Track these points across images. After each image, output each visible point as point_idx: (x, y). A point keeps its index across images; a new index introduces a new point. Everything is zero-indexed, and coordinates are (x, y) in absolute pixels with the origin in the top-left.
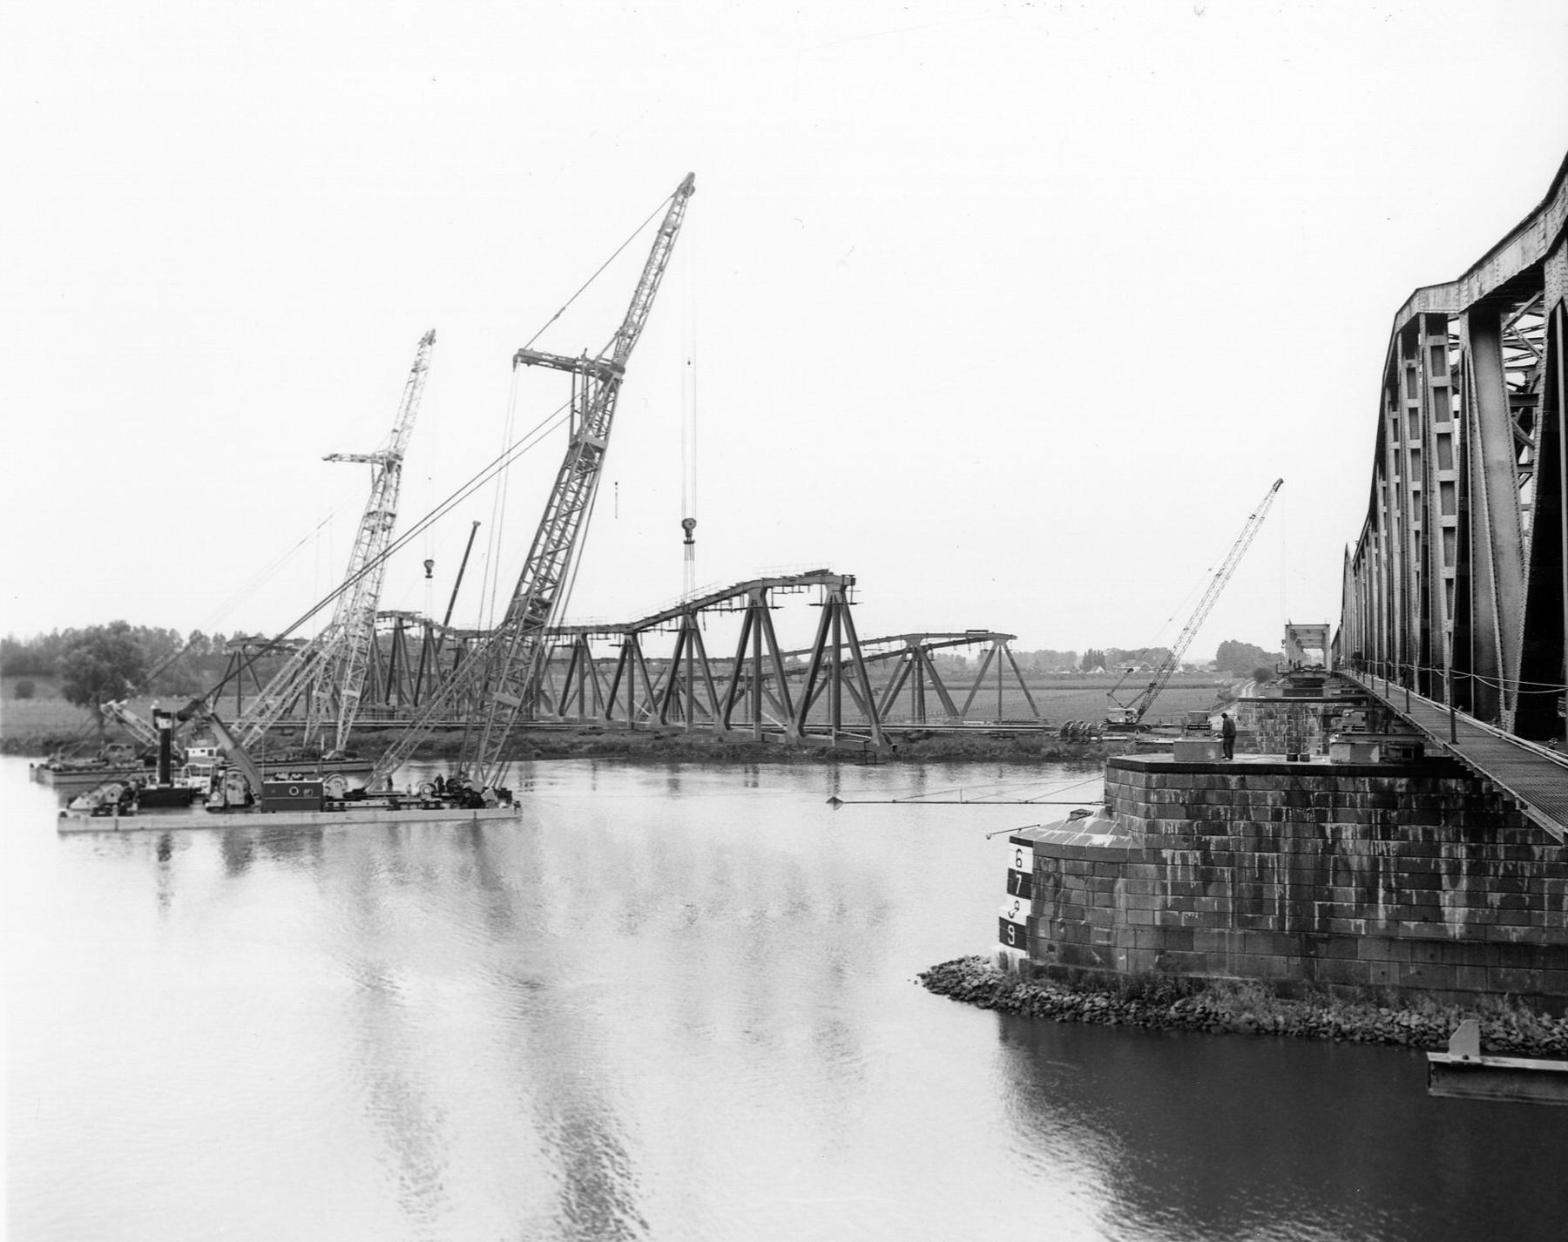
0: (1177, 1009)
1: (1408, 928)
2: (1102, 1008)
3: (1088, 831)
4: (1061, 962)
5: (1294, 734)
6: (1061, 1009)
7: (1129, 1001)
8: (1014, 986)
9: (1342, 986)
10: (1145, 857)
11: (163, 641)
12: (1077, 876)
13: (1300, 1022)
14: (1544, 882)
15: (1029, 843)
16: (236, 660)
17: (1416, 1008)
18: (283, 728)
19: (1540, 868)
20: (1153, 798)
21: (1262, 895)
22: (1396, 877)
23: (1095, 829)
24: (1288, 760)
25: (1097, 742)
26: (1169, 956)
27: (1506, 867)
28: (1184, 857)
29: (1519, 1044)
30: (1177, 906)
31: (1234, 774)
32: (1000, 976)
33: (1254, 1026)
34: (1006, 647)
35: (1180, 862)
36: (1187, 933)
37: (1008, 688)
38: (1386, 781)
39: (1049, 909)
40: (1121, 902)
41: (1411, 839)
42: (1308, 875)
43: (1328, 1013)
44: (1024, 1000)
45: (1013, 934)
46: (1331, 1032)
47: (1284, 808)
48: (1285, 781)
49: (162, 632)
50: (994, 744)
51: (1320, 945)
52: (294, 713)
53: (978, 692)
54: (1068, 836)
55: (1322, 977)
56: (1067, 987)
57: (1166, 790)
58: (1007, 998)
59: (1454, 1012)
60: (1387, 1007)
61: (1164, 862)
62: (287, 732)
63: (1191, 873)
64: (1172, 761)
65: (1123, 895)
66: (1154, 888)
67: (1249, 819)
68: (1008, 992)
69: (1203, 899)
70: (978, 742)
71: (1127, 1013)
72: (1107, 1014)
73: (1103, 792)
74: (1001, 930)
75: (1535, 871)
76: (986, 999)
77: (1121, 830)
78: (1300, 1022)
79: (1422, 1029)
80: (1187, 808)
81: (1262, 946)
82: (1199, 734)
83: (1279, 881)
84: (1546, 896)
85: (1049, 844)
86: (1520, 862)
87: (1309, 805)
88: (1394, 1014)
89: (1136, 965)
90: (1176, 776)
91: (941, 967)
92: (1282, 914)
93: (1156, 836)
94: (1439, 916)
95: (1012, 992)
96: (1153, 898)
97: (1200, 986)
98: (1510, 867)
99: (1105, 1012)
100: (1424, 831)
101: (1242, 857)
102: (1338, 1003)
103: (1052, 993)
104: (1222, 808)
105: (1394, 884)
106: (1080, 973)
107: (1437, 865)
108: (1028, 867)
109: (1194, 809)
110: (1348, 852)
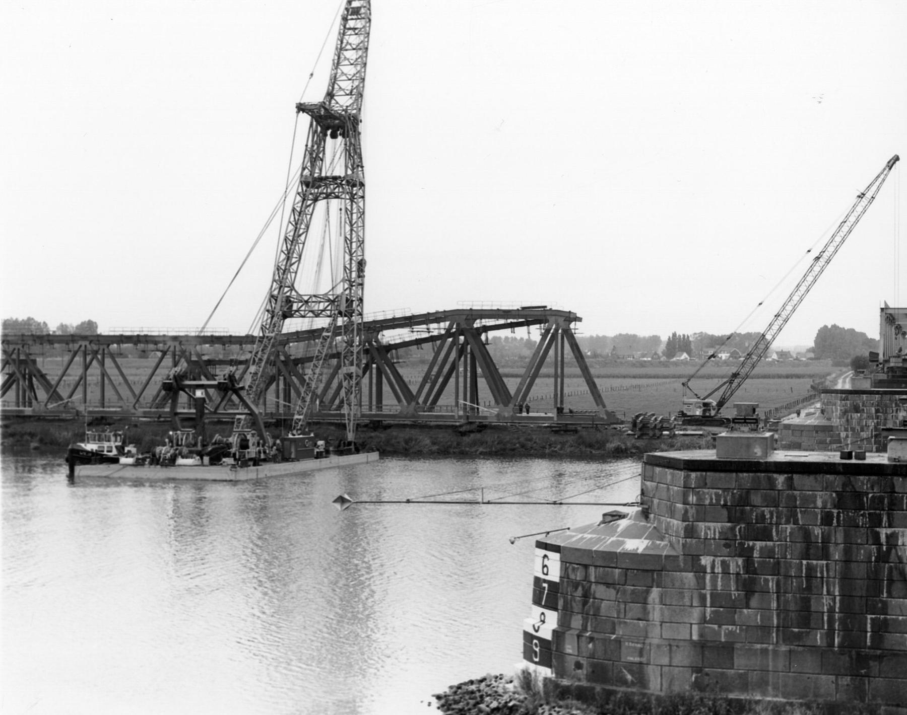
4: (588, 680)
9: (894, 709)
10: (682, 565)
12: (608, 585)
15: (556, 549)
20: (692, 499)
21: (810, 606)
23: (630, 533)
24: (842, 458)
26: (707, 674)
28: (724, 565)
30: (717, 619)
32: (522, 697)
35: (720, 570)
36: (727, 649)
39: (577, 622)
40: (656, 614)
42: (860, 588)
45: (537, 650)
47: (835, 511)
48: (837, 481)
51: (871, 663)
54: (599, 540)
55: (874, 697)
56: (594, 709)
57: (706, 491)
64: (714, 458)
65: (658, 607)
67: (796, 522)
69: (745, 611)
73: (639, 492)
77: (658, 534)
81: (810, 663)
82: (745, 428)
83: (828, 591)
85: (576, 549)
89: (671, 684)
90: (717, 475)
91: (459, 687)
92: (831, 630)
93: (694, 541)
96: (689, 609)
101: (789, 566)
104: (766, 511)
106: (610, 693)
108: (554, 575)
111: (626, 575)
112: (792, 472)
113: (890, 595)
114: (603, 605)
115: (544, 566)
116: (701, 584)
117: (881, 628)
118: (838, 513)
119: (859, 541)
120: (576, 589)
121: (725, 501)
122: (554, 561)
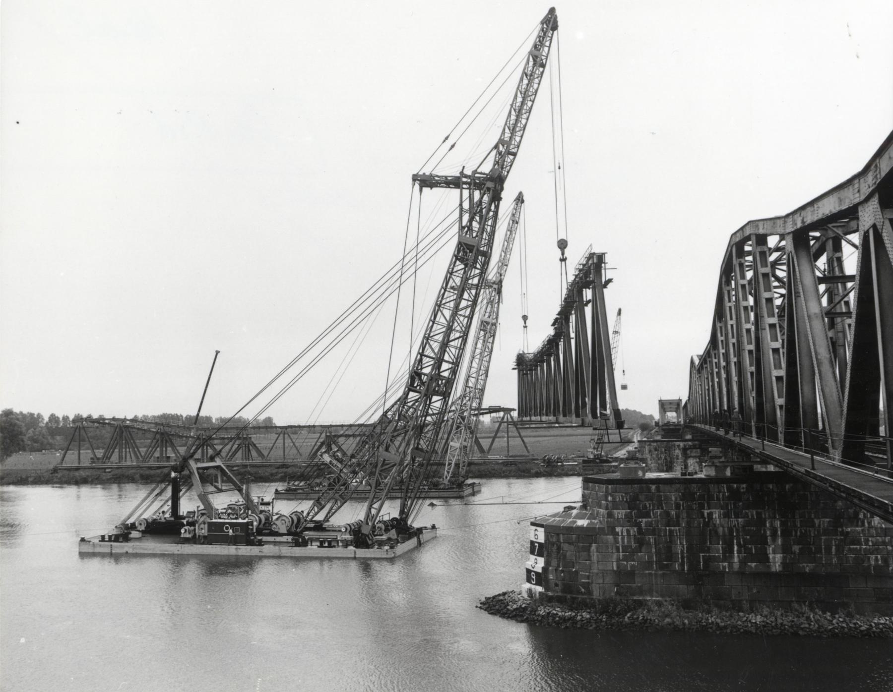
0: (629, 618)
1: (751, 567)
2: (587, 619)
3: (574, 518)
5: (669, 459)
6: (564, 620)
7: (601, 614)
8: (537, 608)
10: (606, 532)
11: (32, 420)
12: (570, 543)
13: (697, 622)
14: (822, 539)
16: (78, 430)
17: (758, 612)
18: (105, 469)
19: (819, 532)
20: (610, 498)
22: (743, 539)
25: (562, 466)
26: (622, 587)
27: (801, 532)
28: (628, 532)
29: (816, 630)
30: (626, 558)
31: (653, 484)
32: (528, 602)
33: (672, 626)
34: (510, 415)
35: (626, 534)
36: (631, 574)
37: (511, 437)
38: (735, 486)
39: (554, 563)
40: (595, 558)
41: (750, 517)
43: (712, 617)
44: (543, 616)
46: (714, 628)
47: (681, 502)
49: (32, 415)
50: (504, 469)
52: (111, 460)
53: (497, 440)
54: (563, 521)
58: (533, 615)
59: (779, 613)
60: (742, 612)
61: (617, 534)
62: (107, 470)
63: (632, 540)
65: (595, 554)
66: (612, 549)
67: (662, 508)
68: (534, 611)
69: (639, 554)
70: (496, 467)
71: (601, 621)
72: (590, 622)
74: (527, 575)
75: (816, 533)
76: (522, 616)
78: (697, 622)
79: (763, 624)
80: (629, 504)
82: (633, 462)
83: (680, 543)
84: (823, 546)
86: (808, 529)
87: (694, 499)
88: (747, 616)
89: (604, 593)
91: (494, 597)
93: (612, 520)
94: (767, 559)
95: (536, 611)
97: (641, 604)
98: (803, 531)
99: (589, 621)
100: (757, 513)
102: (715, 610)
103: (558, 611)
105: (742, 542)
106: (574, 599)
107: (765, 532)
108: (541, 538)
109: (632, 504)
110: (717, 526)
111: (579, 538)
112: (659, 484)
113: (711, 543)
114: (568, 554)
115: (536, 535)
116: (616, 541)
117: (707, 560)
118: (683, 503)
119: (694, 517)
120: (553, 545)
121: (627, 499)
122: (541, 533)
